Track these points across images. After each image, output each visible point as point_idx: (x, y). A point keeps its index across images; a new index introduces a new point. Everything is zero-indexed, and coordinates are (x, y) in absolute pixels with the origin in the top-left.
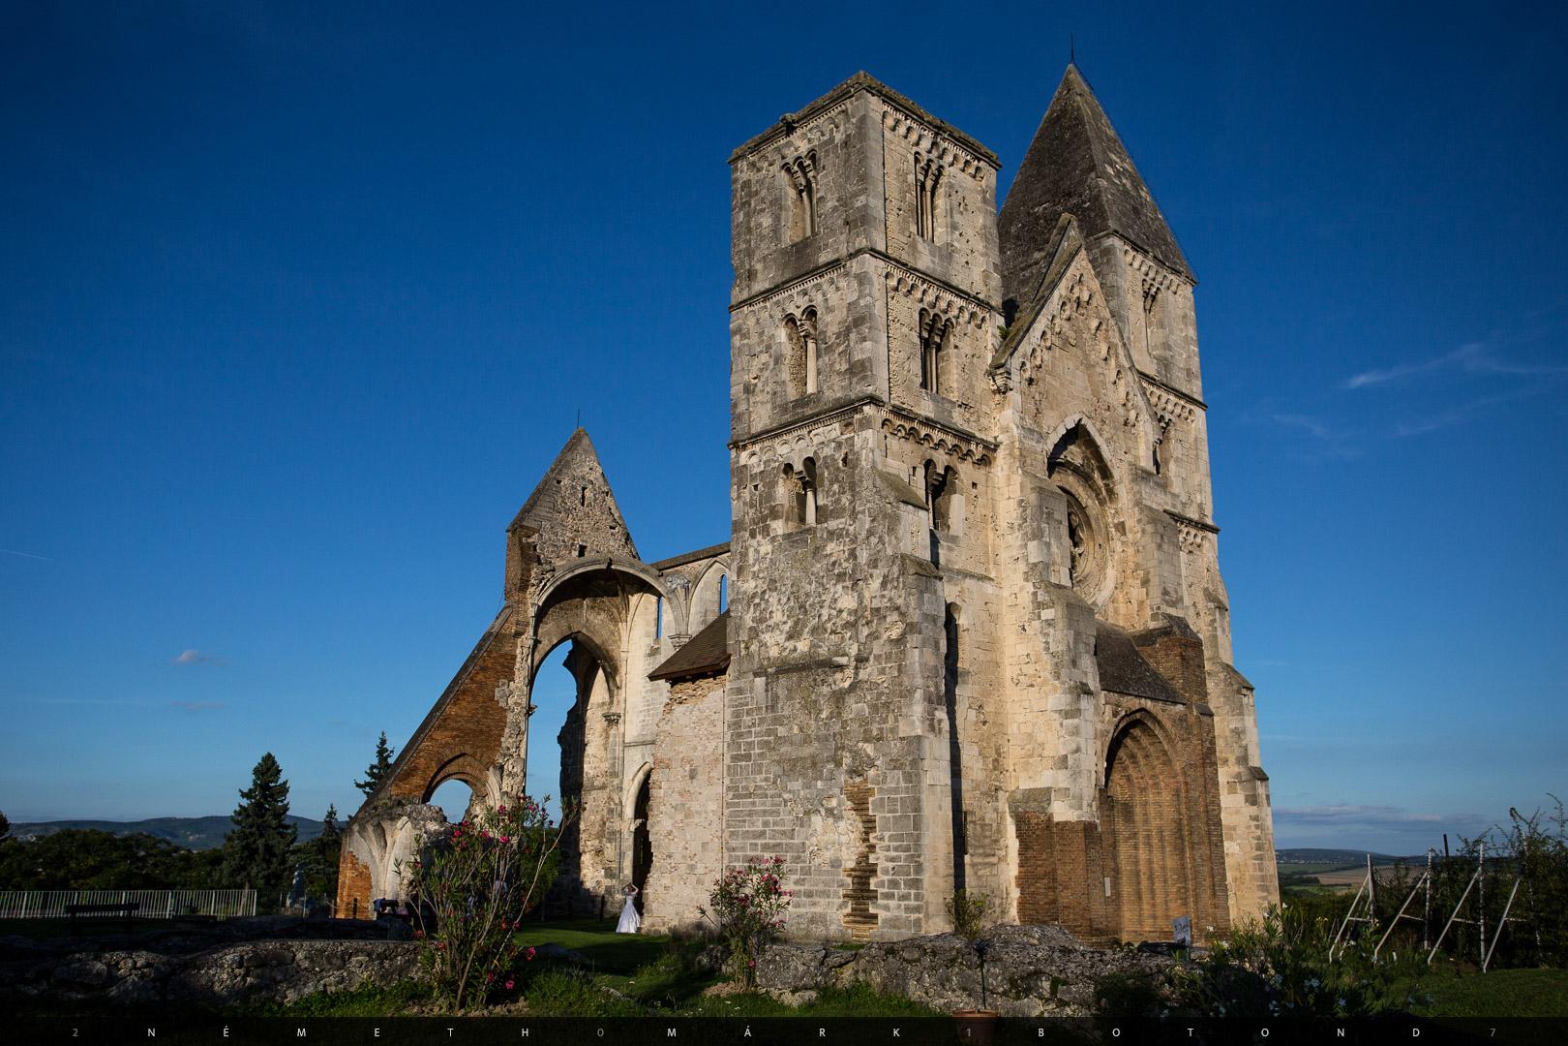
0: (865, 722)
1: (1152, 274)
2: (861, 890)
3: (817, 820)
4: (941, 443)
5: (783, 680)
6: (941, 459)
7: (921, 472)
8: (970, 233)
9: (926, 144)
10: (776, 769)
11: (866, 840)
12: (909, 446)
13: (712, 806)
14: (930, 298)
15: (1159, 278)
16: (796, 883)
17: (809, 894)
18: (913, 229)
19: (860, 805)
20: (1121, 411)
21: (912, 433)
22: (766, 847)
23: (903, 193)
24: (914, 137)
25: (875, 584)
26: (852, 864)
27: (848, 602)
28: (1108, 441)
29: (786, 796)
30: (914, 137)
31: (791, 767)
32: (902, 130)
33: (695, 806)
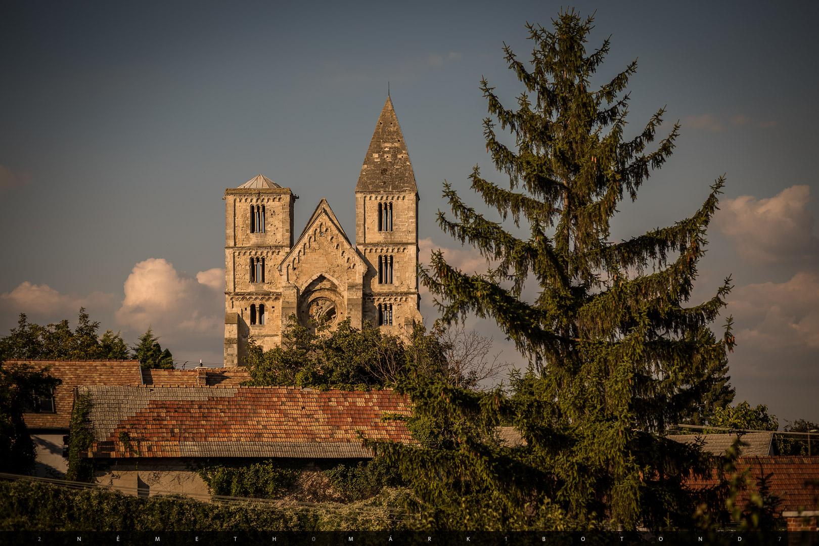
1: (385, 198)
4: (256, 299)
6: (257, 303)
7: (249, 309)
8: (276, 223)
9: (254, 200)
12: (243, 303)
14: (253, 253)
15: (390, 198)
18: (249, 232)
20: (346, 265)
21: (243, 299)
23: (244, 221)
24: (249, 200)
28: (337, 278)
30: (249, 200)
32: (244, 200)
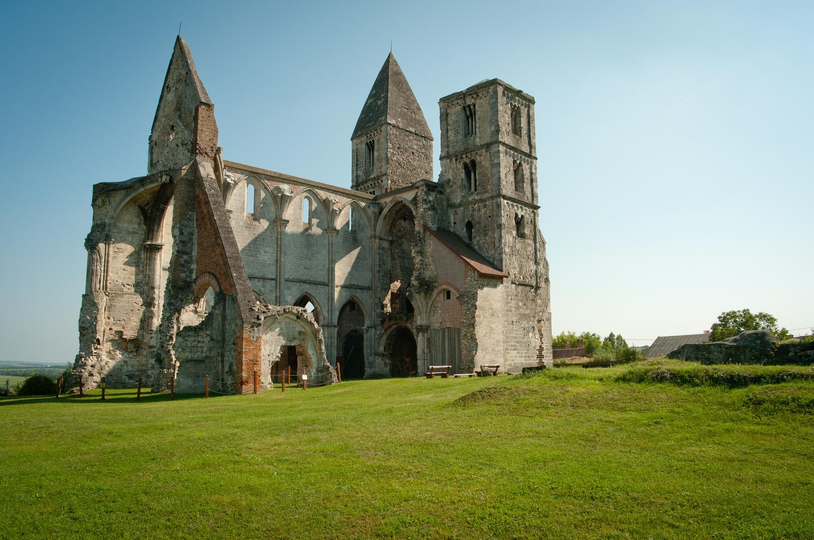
0: (540, 306)
2: (540, 356)
3: (531, 334)
5: (520, 287)
10: (519, 316)
11: (541, 341)
13: (500, 327)
16: (525, 353)
17: (529, 357)
19: (540, 331)
22: (517, 342)
25: (542, 266)
26: (538, 348)
27: (533, 267)
29: (522, 326)
31: (524, 317)
33: (494, 326)
